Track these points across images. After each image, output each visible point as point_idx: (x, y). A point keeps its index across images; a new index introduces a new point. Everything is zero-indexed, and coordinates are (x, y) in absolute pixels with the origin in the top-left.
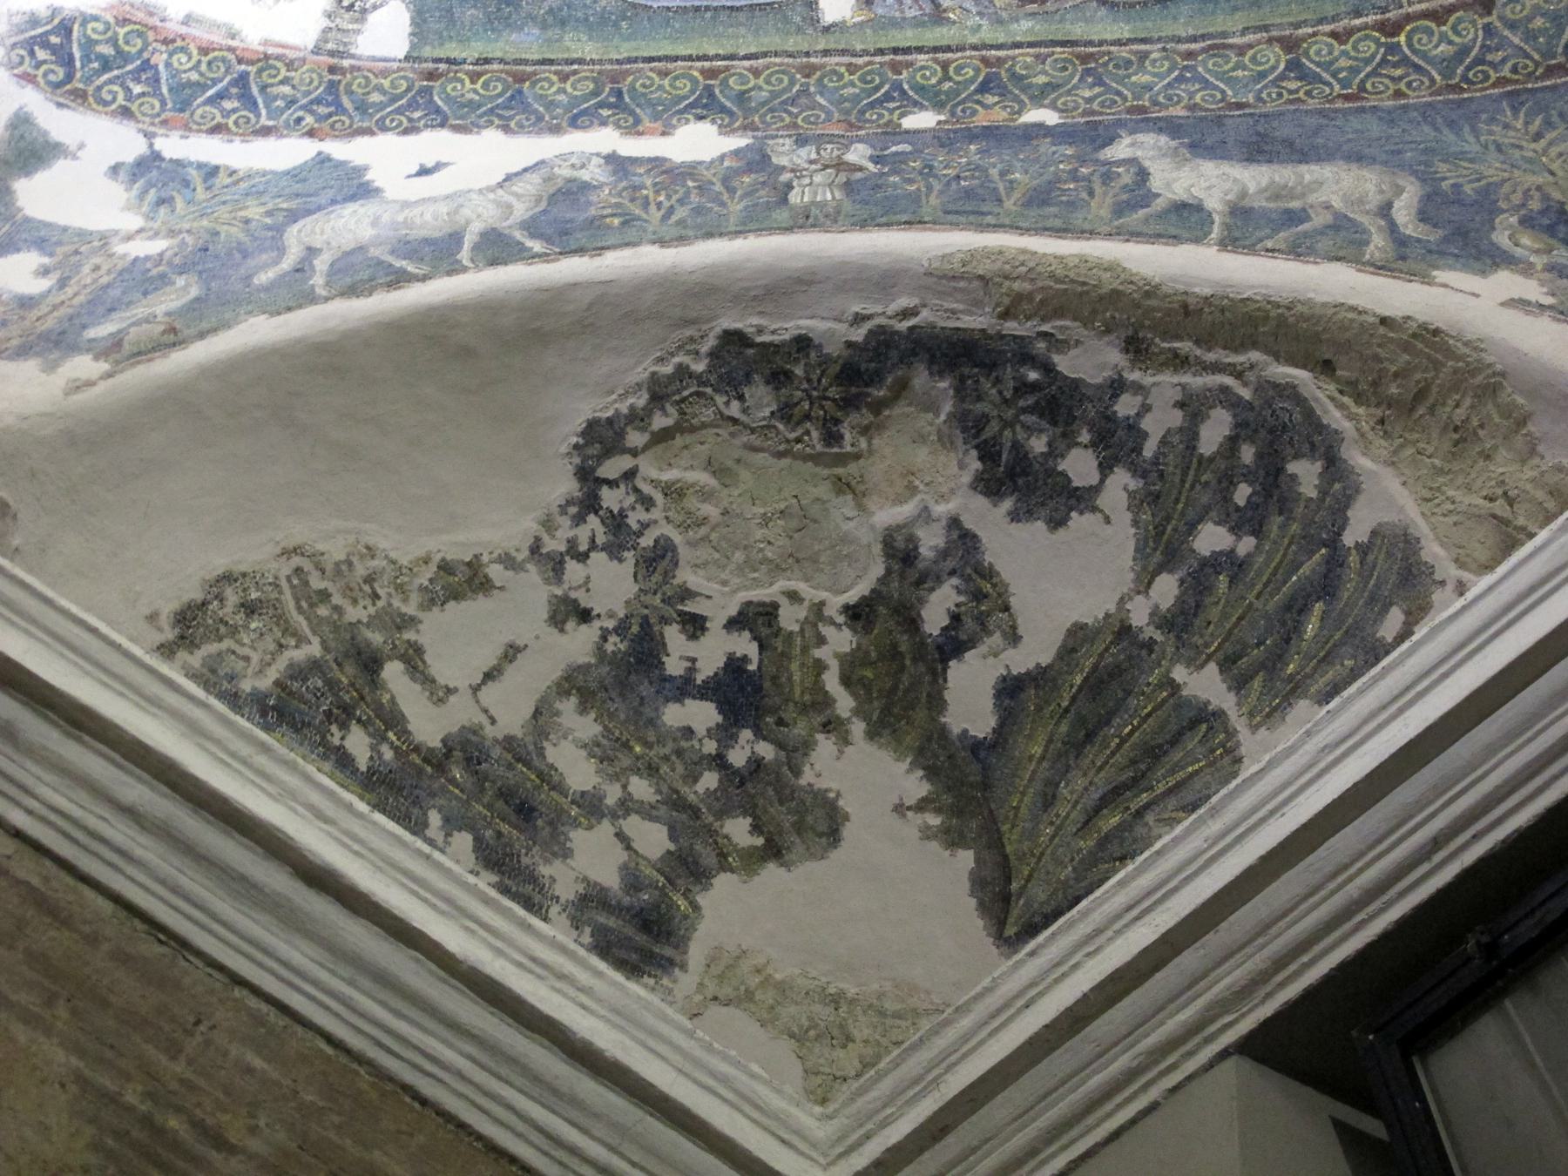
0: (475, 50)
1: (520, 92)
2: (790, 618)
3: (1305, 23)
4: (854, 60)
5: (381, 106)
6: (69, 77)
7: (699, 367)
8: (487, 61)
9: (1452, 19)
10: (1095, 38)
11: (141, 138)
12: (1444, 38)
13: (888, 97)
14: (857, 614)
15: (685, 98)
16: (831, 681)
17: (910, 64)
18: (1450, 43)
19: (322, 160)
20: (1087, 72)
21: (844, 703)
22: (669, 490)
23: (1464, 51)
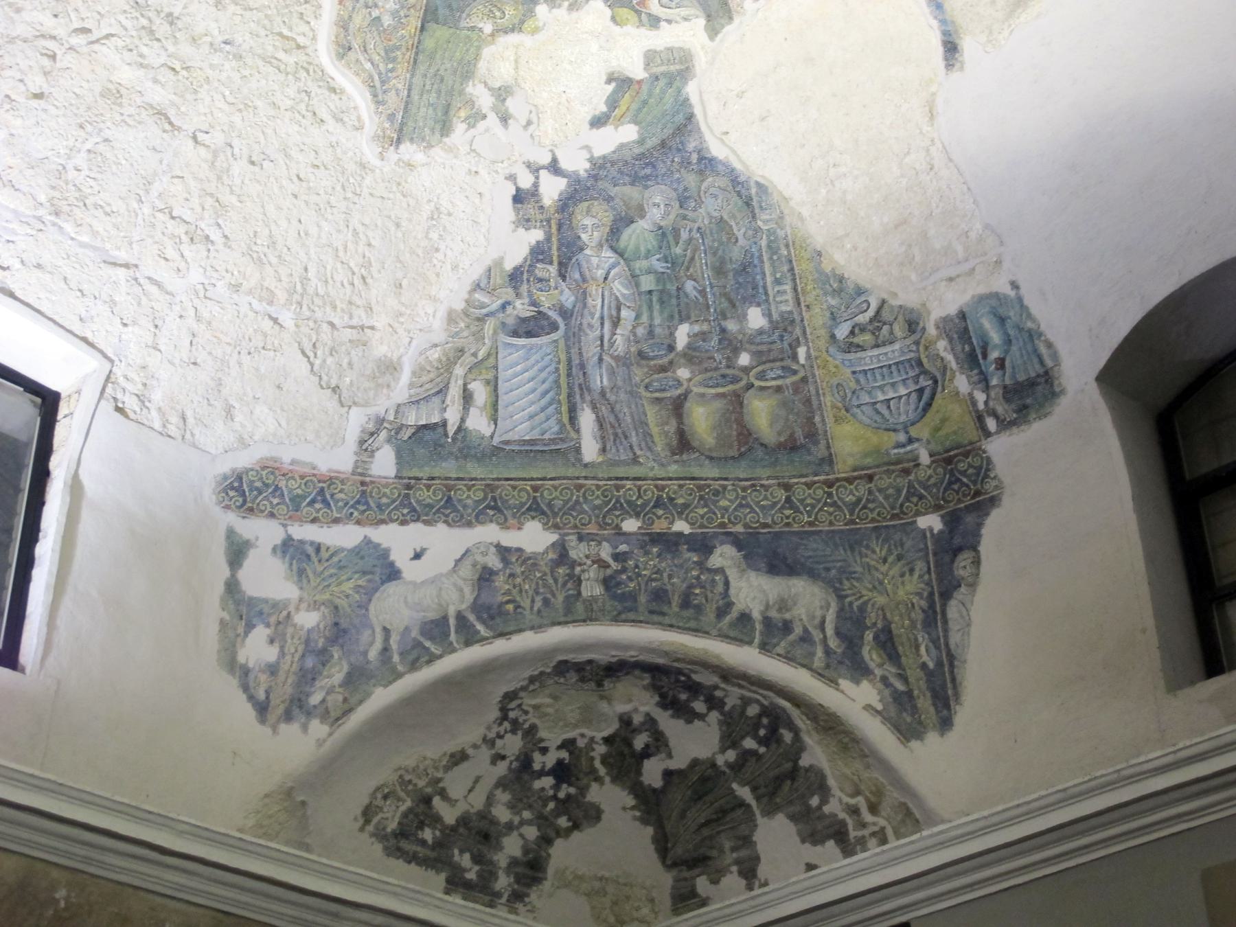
0: (424, 473)
1: (450, 498)
2: (581, 743)
3: (794, 477)
4: (601, 483)
5: (388, 505)
6: (245, 502)
7: (549, 670)
8: (433, 479)
10: (704, 476)
11: (282, 529)
12: (851, 493)
13: (614, 508)
14: (607, 740)
15: (525, 503)
16: (597, 764)
17: (623, 486)
19: (367, 541)
20: (701, 498)
21: (602, 771)
22: (536, 707)
23: (859, 500)
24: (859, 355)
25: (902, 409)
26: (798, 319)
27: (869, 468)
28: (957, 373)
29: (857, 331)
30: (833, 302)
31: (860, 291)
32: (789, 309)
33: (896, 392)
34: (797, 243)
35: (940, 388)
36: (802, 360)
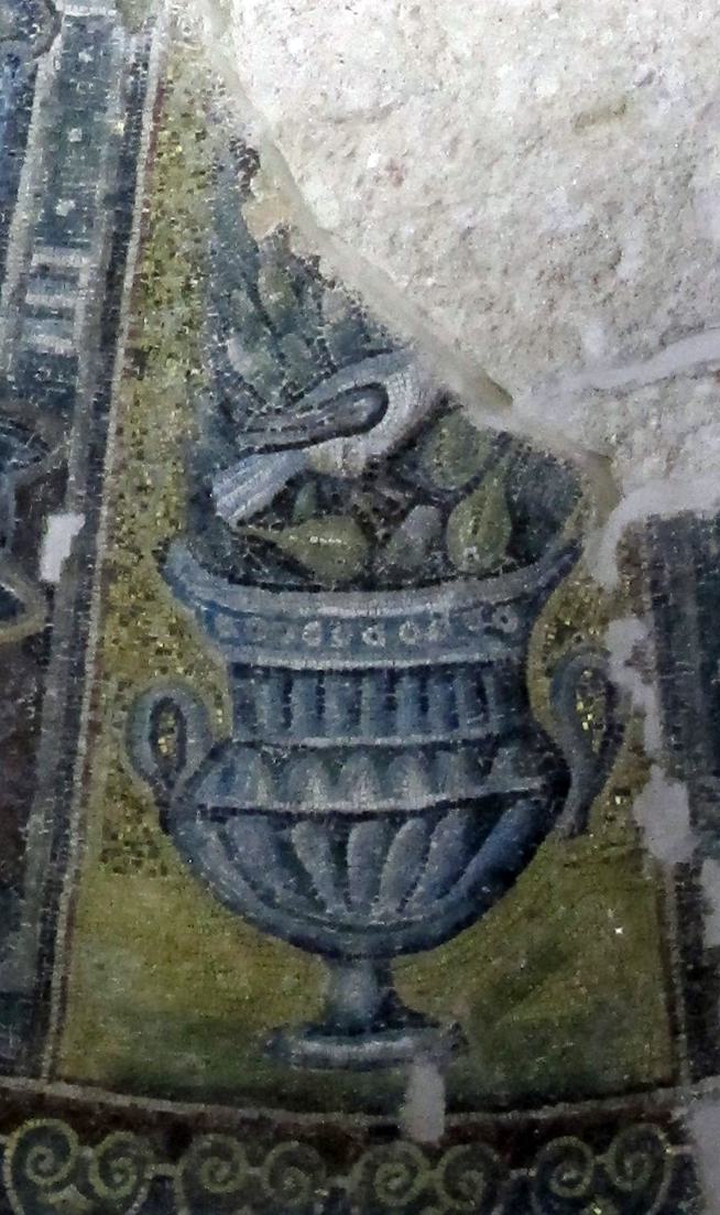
9: (109, 1141)
12: (78, 1176)
18: (87, 1190)
24: (283, 602)
25: (388, 872)
26: (86, 393)
27: (182, 1094)
28: (657, 772)
29: (303, 500)
30: (242, 360)
31: (363, 341)
32: (62, 347)
33: (385, 790)
34: (178, 98)
35: (567, 819)
36: (51, 568)
